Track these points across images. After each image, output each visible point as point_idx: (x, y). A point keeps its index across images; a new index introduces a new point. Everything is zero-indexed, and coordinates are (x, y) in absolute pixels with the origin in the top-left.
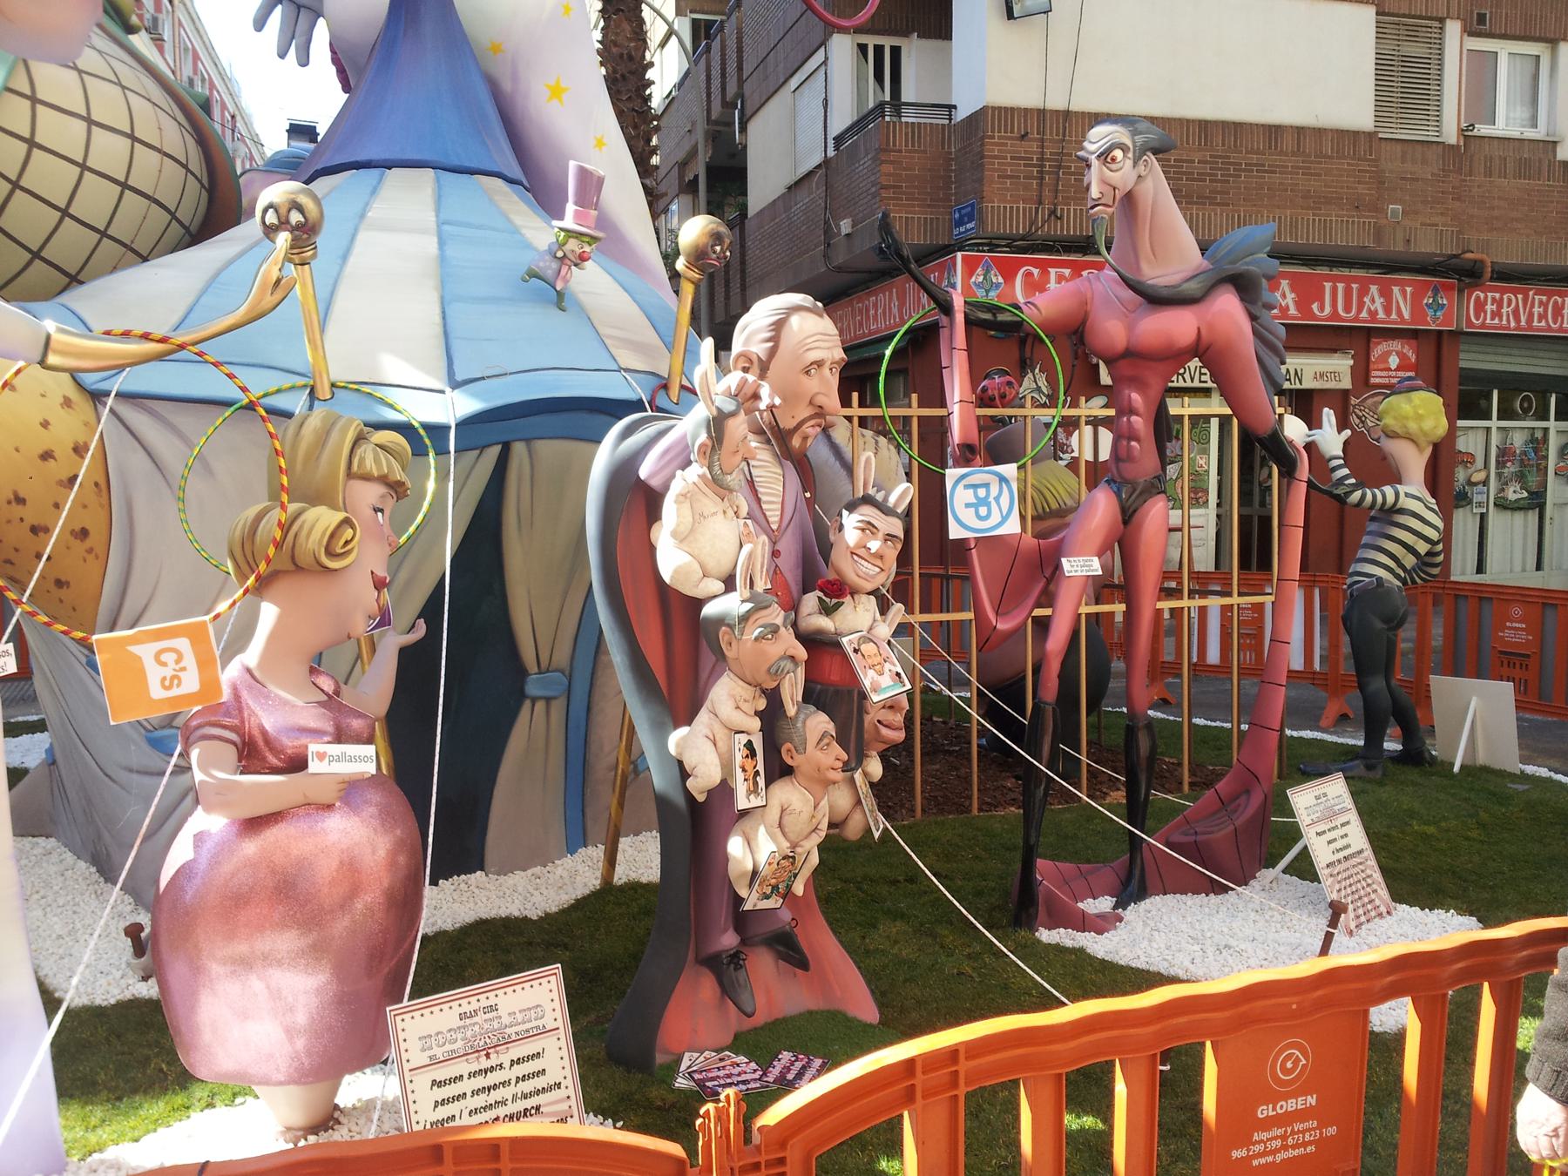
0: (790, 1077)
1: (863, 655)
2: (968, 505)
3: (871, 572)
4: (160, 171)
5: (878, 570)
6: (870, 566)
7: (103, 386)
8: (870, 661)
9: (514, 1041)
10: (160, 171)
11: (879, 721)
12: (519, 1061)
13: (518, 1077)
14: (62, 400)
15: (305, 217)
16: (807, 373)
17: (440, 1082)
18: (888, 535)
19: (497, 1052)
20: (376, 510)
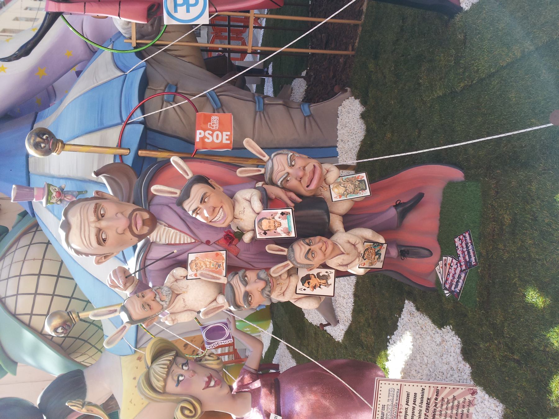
0: (468, 260)
1: (268, 230)
2: (188, 11)
3: (222, 215)
4: (51, 260)
5: (221, 209)
6: (218, 216)
7: (133, 351)
8: (272, 228)
9: (399, 402)
10: (51, 260)
11: (308, 187)
12: (407, 402)
13: (413, 404)
14: (139, 361)
15: (59, 327)
16: (104, 240)
17: (407, 402)
18: (201, 202)
19: (401, 409)
20: (179, 382)
